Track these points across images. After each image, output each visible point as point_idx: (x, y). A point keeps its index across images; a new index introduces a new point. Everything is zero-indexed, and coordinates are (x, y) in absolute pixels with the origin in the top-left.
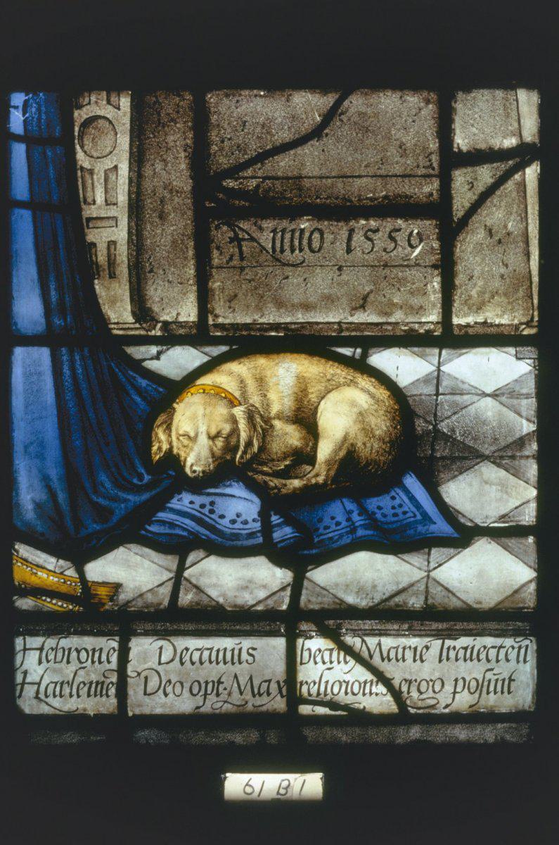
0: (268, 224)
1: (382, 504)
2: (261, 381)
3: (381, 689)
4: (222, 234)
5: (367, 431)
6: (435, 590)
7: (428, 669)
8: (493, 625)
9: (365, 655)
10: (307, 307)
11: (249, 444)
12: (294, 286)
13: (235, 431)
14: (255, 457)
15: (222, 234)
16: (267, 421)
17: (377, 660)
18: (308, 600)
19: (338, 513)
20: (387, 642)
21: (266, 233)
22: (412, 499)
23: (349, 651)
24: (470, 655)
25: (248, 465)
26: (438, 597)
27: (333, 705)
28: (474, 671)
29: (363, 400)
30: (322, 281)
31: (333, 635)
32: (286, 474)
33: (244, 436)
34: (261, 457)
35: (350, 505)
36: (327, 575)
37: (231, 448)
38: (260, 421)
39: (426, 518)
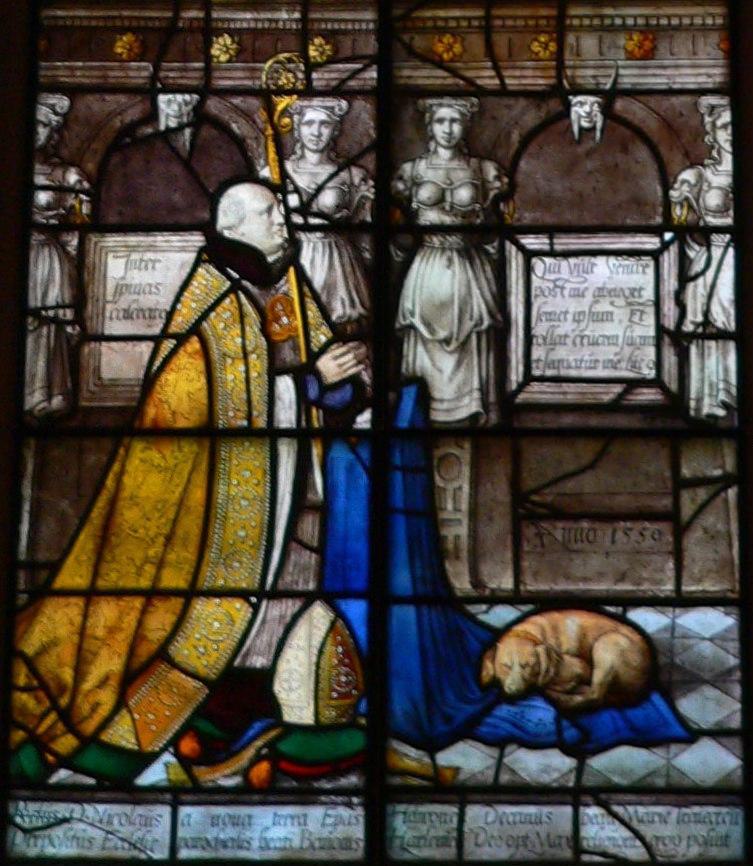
0: (560, 525)
1: (637, 715)
2: (555, 629)
3: (638, 843)
4: (529, 531)
5: (626, 663)
6: (673, 773)
7: (667, 831)
8: (713, 798)
9: (626, 819)
10: (585, 580)
11: (547, 671)
12: (577, 566)
13: (538, 663)
14: (552, 679)
15: (529, 531)
16: (559, 655)
17: (635, 824)
18: (588, 781)
19: (606, 721)
20: (641, 810)
21: (559, 530)
22: (657, 710)
23: (615, 816)
24: (699, 820)
25: (547, 686)
26: (676, 780)
27: (604, 854)
28: (701, 831)
29: (623, 642)
30: (596, 562)
31: (604, 805)
32: (571, 692)
33: (544, 665)
34: (555, 680)
35: (615, 714)
36: (599, 763)
37: (535, 674)
38: (555, 656)
39: (666, 723)
